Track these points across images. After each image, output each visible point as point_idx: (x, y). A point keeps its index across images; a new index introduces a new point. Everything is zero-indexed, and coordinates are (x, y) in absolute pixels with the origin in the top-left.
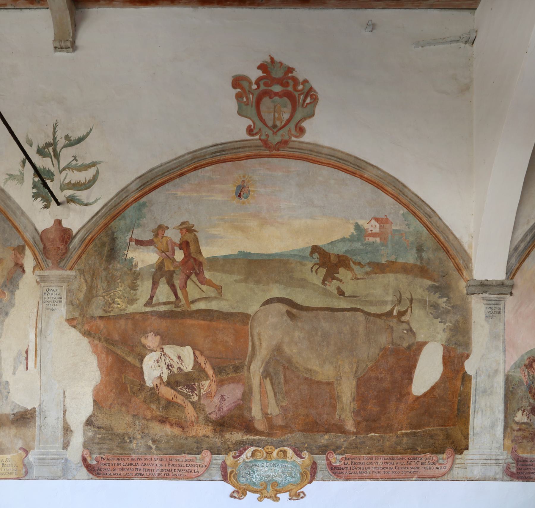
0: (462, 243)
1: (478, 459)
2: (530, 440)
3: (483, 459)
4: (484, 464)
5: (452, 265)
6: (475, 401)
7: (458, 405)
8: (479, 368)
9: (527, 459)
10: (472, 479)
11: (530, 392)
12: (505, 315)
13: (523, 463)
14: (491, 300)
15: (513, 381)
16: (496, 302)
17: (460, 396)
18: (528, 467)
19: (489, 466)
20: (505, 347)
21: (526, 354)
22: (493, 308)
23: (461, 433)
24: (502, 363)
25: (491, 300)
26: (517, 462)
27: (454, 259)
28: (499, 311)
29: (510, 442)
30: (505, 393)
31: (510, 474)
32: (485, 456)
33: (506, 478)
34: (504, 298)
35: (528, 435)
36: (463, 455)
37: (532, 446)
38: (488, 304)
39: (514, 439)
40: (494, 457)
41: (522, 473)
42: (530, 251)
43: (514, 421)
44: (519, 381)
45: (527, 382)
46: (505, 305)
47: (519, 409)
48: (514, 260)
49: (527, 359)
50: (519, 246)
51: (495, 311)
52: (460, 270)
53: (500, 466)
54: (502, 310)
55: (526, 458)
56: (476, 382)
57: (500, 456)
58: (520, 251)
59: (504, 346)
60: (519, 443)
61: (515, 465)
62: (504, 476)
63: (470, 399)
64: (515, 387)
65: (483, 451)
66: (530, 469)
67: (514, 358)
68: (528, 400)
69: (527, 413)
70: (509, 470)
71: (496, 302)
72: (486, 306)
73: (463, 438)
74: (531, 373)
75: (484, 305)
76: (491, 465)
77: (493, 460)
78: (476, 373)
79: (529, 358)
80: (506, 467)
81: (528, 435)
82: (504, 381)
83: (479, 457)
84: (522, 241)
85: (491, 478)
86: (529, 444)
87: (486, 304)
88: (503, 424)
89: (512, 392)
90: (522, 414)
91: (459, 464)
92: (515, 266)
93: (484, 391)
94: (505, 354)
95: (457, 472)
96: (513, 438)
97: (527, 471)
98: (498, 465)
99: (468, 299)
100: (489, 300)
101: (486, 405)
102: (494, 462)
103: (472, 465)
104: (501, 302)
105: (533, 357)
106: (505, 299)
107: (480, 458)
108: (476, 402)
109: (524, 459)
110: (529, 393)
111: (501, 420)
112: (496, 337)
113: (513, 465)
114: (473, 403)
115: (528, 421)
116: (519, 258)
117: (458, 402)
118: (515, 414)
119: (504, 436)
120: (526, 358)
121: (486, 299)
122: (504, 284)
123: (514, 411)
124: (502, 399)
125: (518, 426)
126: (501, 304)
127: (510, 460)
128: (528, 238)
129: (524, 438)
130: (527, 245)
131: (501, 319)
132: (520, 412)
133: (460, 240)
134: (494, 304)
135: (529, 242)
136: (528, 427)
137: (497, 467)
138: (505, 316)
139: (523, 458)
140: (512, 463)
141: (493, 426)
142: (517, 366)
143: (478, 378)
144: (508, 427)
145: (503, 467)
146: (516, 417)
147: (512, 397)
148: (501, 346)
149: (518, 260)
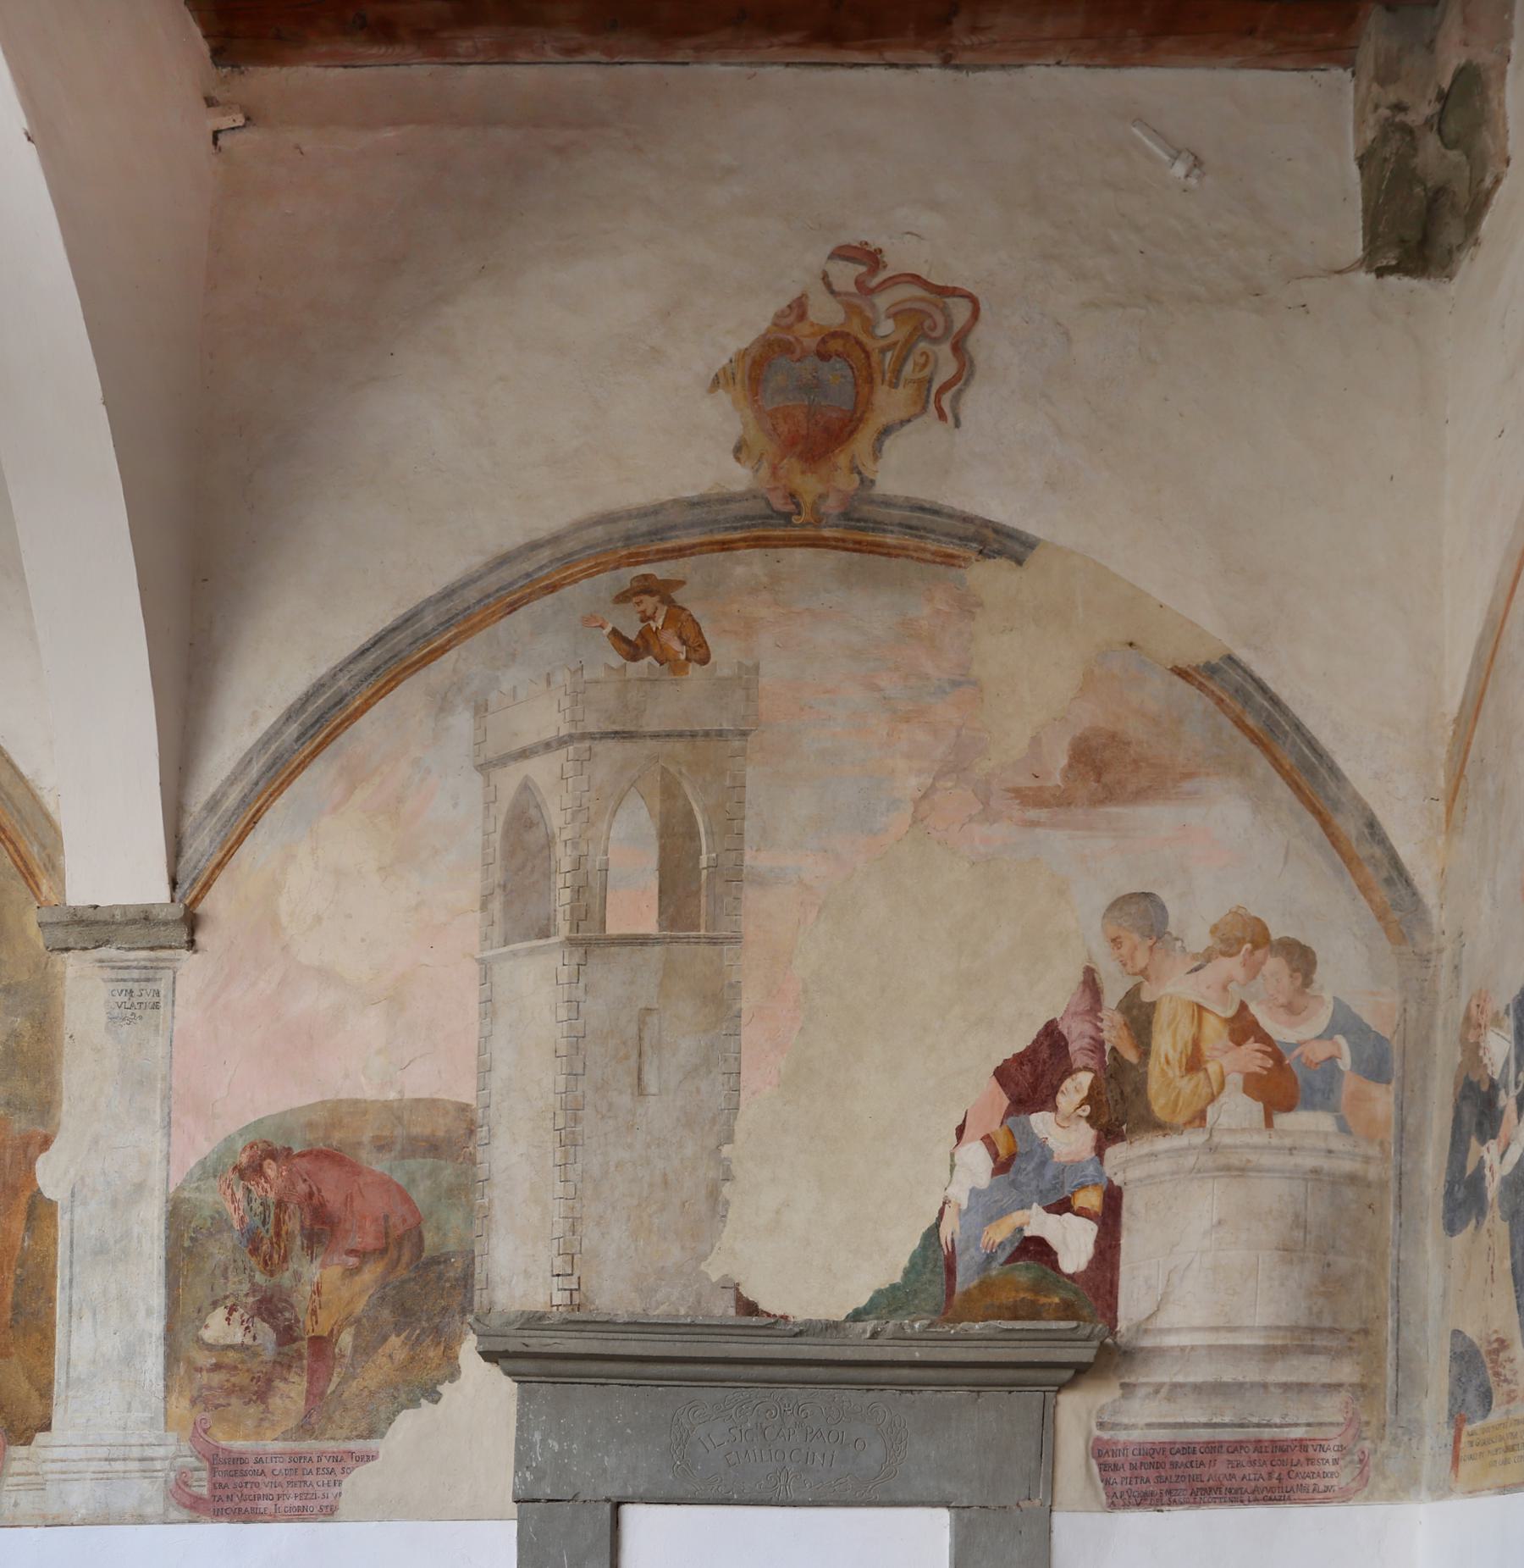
1: (81, 1460)
2: (254, 1398)
3: (100, 1460)
4: (104, 1472)
5: (8, 861)
6: (71, 1281)
7: (15, 1294)
8: (82, 1178)
9: (244, 1457)
10: (61, 1521)
11: (254, 1251)
12: (173, 1013)
13: (232, 1467)
14: (127, 968)
15: (193, 1217)
16: (144, 974)
17: (21, 1266)
18: (248, 1478)
19: (118, 1478)
20: (169, 1113)
21: (241, 1135)
22: (136, 993)
23: (29, 1378)
24: (160, 1162)
25: (127, 968)
26: (212, 1464)
27: (12, 843)
28: (156, 999)
29: (185, 1403)
30: (167, 1254)
31: (188, 1503)
32: (105, 1449)
33: (176, 1512)
34: (171, 960)
35: (246, 1381)
36: (32, 1448)
37: (262, 1416)
38: (118, 980)
39: (200, 1396)
40: (136, 1452)
41: (229, 1498)
42: (258, 811)
43: (199, 1340)
44: (213, 1218)
45: (242, 1219)
46: (174, 982)
49: (244, 1150)
50: (224, 794)
51: (141, 1000)
52: (32, 875)
53: (156, 1477)
54: (165, 996)
55: (240, 1453)
56: (72, 1220)
57: (157, 1448)
58: (225, 811)
59: (167, 1110)
61: (204, 1474)
62: (171, 1509)
63: (54, 1276)
65: (100, 1434)
66: (257, 1485)
67: (199, 1145)
68: (246, 1276)
69: (242, 1316)
70: (187, 1490)
71: (144, 974)
72: (111, 986)
73: (34, 1395)
74: (257, 1192)
75: (102, 984)
76: (127, 1475)
77: (134, 1460)
78: (73, 1195)
79: (252, 1147)
80: (176, 1480)
81: (246, 1381)
82: (164, 1217)
83: (87, 1452)
84: (232, 780)
85: (127, 1516)
87: (112, 980)
88: (161, 1350)
90: (228, 1319)
91: (18, 1474)
92: (207, 860)
93: (101, 1250)
94: (169, 1135)
95: (13, 1501)
96: (195, 1394)
97: (245, 1491)
98: (147, 1474)
99: (52, 966)
100: (120, 968)
103: (63, 1476)
104: (160, 974)
105: (265, 1142)
106: (177, 964)
107: (89, 1456)
108: (74, 1284)
109: (236, 1456)
110: (249, 1255)
111: (154, 1339)
114: (63, 1288)
115: (248, 1341)
116: (222, 833)
117: (15, 1283)
118: (203, 1320)
119: (166, 1387)
120: (239, 1145)
122: (151, 917)
123: (199, 1311)
126: (161, 979)
127: (189, 1459)
128: (255, 771)
129: (233, 1392)
130: (251, 791)
131: (161, 1027)
132: (221, 1313)
134: (138, 981)
135: (256, 784)
136: (246, 1358)
138: (173, 1017)
139: (230, 1452)
140: (196, 1469)
141: (130, 1357)
142: (208, 1170)
143: (79, 1211)
146: (206, 1327)
148: (158, 1110)
149: (218, 840)
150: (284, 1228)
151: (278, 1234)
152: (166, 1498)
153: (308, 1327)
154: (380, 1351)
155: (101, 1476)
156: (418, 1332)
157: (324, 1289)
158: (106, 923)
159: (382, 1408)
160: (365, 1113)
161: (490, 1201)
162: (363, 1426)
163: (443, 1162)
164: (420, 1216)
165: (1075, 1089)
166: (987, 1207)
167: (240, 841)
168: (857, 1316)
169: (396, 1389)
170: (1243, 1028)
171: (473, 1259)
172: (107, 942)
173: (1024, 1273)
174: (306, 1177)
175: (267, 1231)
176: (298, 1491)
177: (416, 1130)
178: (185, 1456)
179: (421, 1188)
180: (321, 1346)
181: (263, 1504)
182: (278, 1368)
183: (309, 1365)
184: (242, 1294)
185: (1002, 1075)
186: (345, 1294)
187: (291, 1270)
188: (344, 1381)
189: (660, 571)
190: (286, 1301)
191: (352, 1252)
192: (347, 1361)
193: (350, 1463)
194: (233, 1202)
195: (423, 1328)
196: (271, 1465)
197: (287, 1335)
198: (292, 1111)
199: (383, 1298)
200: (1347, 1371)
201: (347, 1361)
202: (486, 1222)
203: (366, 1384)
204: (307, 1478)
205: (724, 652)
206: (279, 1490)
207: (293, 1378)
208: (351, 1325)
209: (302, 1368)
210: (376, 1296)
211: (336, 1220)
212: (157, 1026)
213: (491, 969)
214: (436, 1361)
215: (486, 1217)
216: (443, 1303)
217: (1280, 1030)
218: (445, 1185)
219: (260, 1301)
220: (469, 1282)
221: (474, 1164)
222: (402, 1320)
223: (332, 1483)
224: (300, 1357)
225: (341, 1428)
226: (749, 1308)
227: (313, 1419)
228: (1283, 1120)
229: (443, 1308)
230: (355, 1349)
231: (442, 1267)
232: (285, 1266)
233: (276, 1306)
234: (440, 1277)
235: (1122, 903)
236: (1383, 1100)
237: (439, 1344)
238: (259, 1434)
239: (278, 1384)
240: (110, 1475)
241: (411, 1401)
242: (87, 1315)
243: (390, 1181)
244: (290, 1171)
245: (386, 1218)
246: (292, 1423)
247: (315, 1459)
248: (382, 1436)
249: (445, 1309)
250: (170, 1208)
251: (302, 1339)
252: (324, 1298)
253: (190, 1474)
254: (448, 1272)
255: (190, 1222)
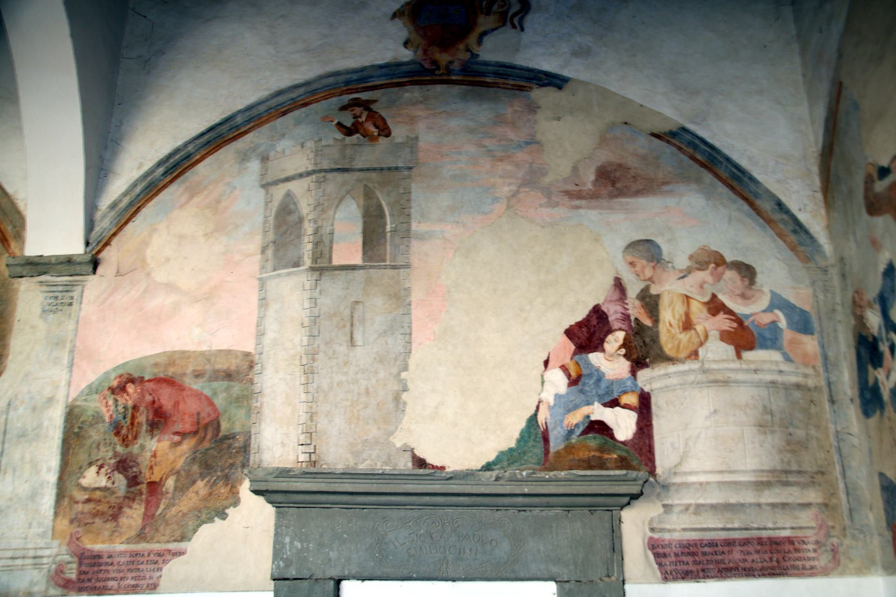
0: (16, 201)
2: (110, 518)
3: (7, 558)
4: (9, 566)
8: (16, 396)
9: (101, 554)
11: (117, 434)
13: (93, 561)
15: (82, 415)
16: (65, 288)
18: (103, 568)
19: (18, 569)
22: (60, 298)
24: (65, 386)
26: (80, 559)
28: (71, 301)
29: (66, 522)
30: (64, 436)
32: (12, 552)
34: (82, 281)
37: (114, 529)
39: (76, 518)
40: (31, 553)
41: (89, 580)
42: (139, 207)
45: (111, 416)
47: (90, 464)
48: (108, 223)
50: (120, 201)
53: (43, 568)
55: (99, 552)
56: (6, 419)
57: (45, 550)
58: (120, 208)
60: (86, 524)
61: (74, 566)
62: (51, 588)
64: (85, 426)
66: (108, 571)
70: (62, 575)
71: (65, 288)
72: (46, 295)
74: (121, 401)
78: (9, 404)
84: (125, 194)
86: (108, 526)
89: (78, 435)
92: (108, 232)
93: (23, 435)
94: (71, 371)
96: (73, 516)
97: (100, 576)
98: (38, 566)
101: (23, 458)
102: (29, 561)
104: (75, 288)
106: (85, 283)
109: (95, 554)
111: (50, 485)
112: (57, 344)
113: (69, 566)
115: (109, 485)
116: (118, 219)
118: (82, 473)
120: (113, 376)
121: (47, 284)
123: (81, 468)
124: (58, 447)
125: (85, 495)
128: (138, 189)
130: (135, 199)
132: (94, 469)
133: (12, 198)
134: (62, 292)
135: (138, 195)
136: (107, 495)
137: (37, 571)
139: (92, 551)
141: (34, 496)
142: (92, 390)
143: (11, 413)
144: (63, 497)
145: (49, 571)
146: (84, 477)
147: (78, 443)
149: (115, 222)
150: (137, 421)
151: (132, 424)
152: (48, 582)
153: (147, 476)
154: (191, 489)
155: (6, 568)
156: (215, 478)
157: (158, 454)
158: (45, 264)
159: (190, 523)
160: (189, 358)
161: (262, 404)
162: (178, 534)
163: (233, 383)
164: (219, 413)
165: (615, 340)
166: (566, 405)
167: (126, 223)
168: (488, 467)
169: (200, 511)
170: (715, 307)
171: (250, 437)
172: (45, 273)
173: (593, 441)
174: (151, 392)
175: (126, 422)
176: (134, 574)
177: (219, 366)
178: (63, 555)
179: (220, 397)
180: (154, 487)
181: (111, 583)
182: (127, 501)
183: (146, 498)
184: (108, 457)
185: (570, 333)
186: (171, 457)
187: (139, 444)
188: (168, 507)
189: (364, 96)
190: (135, 461)
191: (177, 433)
192: (169, 495)
193: (168, 557)
194: (107, 407)
195: (218, 476)
196: (118, 559)
197: (133, 481)
198: (145, 358)
199: (194, 459)
200: (813, 496)
201: (169, 495)
202: (259, 415)
203: (181, 509)
204: (141, 567)
205: (399, 132)
206: (122, 575)
207: (135, 505)
208: (174, 474)
209: (141, 500)
210: (191, 458)
211: (168, 416)
212: (70, 314)
213: (265, 283)
214: (226, 495)
215: (258, 413)
216: (231, 461)
217: (739, 308)
218: (235, 395)
219: (119, 462)
220: (248, 449)
221: (252, 384)
222: (205, 471)
223: (156, 570)
224: (141, 493)
225: (164, 535)
226: (421, 463)
227: (147, 531)
228: (747, 355)
229: (231, 464)
230: (176, 488)
231: (231, 441)
232: (135, 441)
233: (128, 465)
234: (230, 446)
235: (633, 246)
236: (810, 344)
237: (227, 485)
238: (111, 540)
239: (126, 509)
240: (13, 568)
241: (209, 519)
242: (10, 472)
243: (202, 394)
244: (142, 389)
245: (198, 414)
246: (133, 533)
247: (146, 555)
248: (190, 540)
249: (232, 465)
250: (68, 411)
251: (143, 483)
252: (158, 459)
253: (65, 566)
254: (235, 443)
255: (80, 418)
